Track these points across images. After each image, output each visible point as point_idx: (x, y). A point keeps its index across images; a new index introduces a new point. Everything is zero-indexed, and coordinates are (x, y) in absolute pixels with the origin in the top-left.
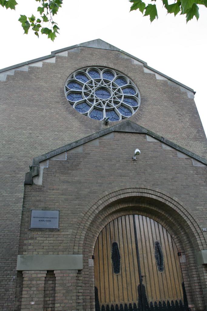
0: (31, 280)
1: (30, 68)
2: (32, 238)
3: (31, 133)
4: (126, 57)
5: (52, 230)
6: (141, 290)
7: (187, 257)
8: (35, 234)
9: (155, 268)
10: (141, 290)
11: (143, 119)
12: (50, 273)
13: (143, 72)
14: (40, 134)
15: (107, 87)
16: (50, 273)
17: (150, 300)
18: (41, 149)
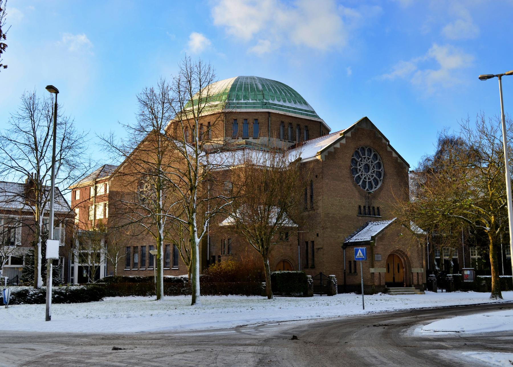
0: (376, 275)
1: (335, 148)
2: (376, 263)
3: (339, 200)
4: (380, 136)
5: (379, 261)
6: (394, 278)
7: (406, 269)
8: (376, 262)
9: (397, 272)
10: (394, 278)
11: (384, 189)
12: (380, 273)
13: (386, 149)
14: (344, 200)
15: (371, 166)
16: (380, 273)
17: (395, 281)
18: (345, 210)
